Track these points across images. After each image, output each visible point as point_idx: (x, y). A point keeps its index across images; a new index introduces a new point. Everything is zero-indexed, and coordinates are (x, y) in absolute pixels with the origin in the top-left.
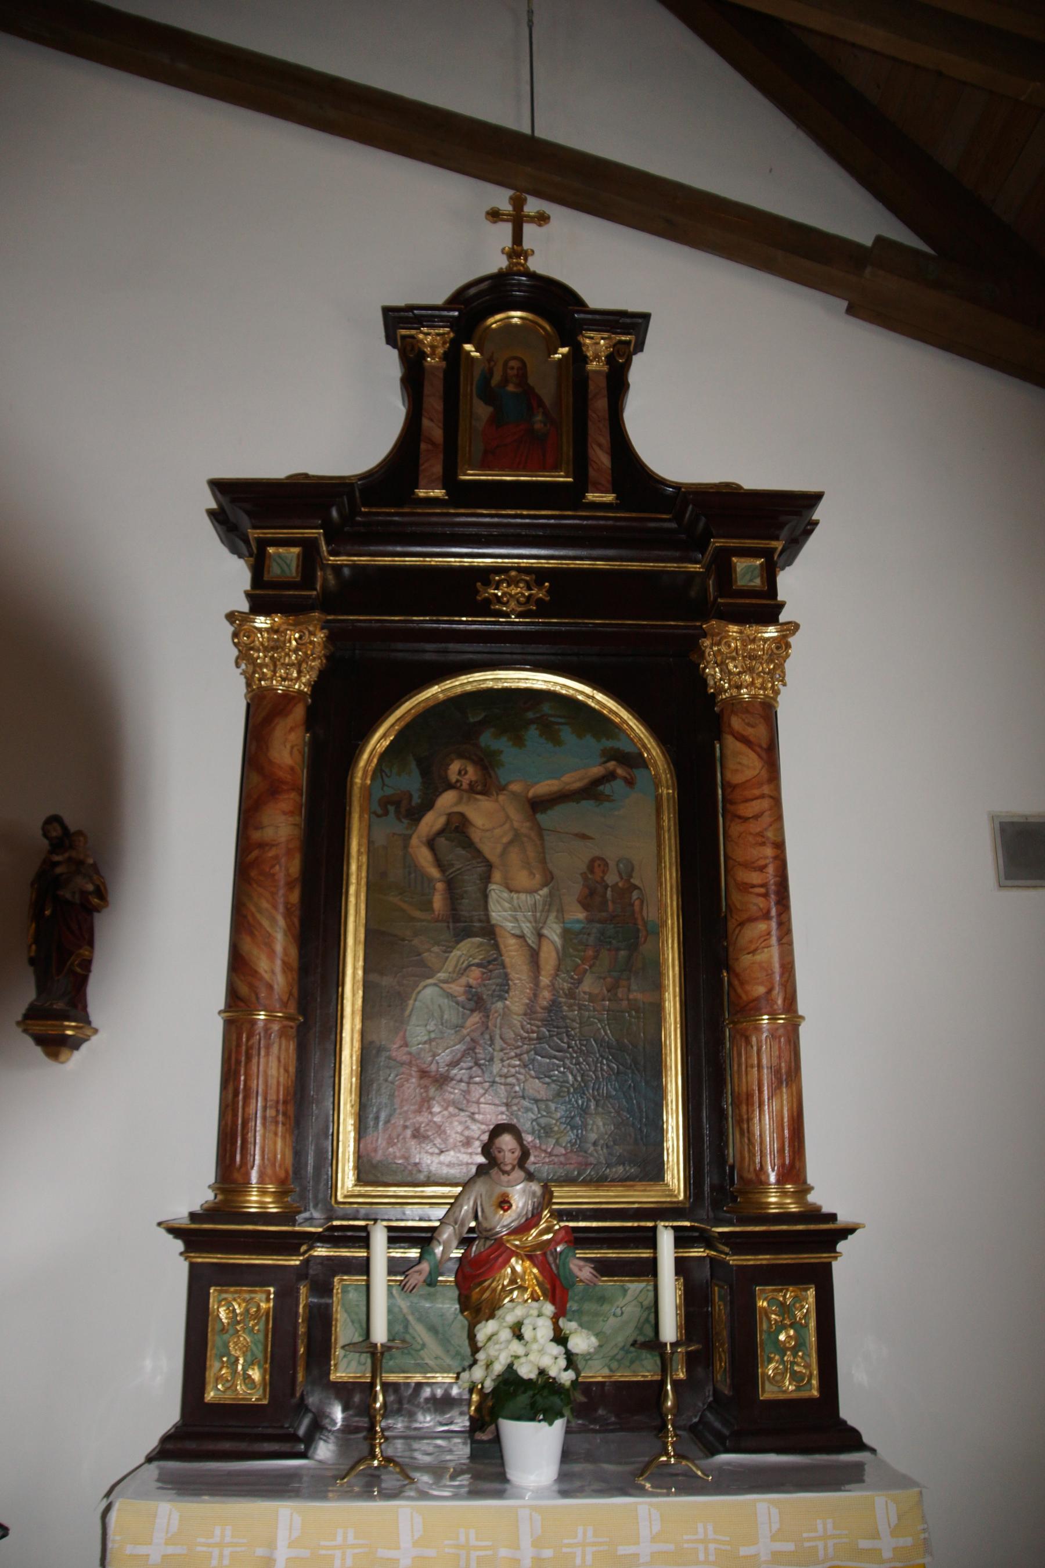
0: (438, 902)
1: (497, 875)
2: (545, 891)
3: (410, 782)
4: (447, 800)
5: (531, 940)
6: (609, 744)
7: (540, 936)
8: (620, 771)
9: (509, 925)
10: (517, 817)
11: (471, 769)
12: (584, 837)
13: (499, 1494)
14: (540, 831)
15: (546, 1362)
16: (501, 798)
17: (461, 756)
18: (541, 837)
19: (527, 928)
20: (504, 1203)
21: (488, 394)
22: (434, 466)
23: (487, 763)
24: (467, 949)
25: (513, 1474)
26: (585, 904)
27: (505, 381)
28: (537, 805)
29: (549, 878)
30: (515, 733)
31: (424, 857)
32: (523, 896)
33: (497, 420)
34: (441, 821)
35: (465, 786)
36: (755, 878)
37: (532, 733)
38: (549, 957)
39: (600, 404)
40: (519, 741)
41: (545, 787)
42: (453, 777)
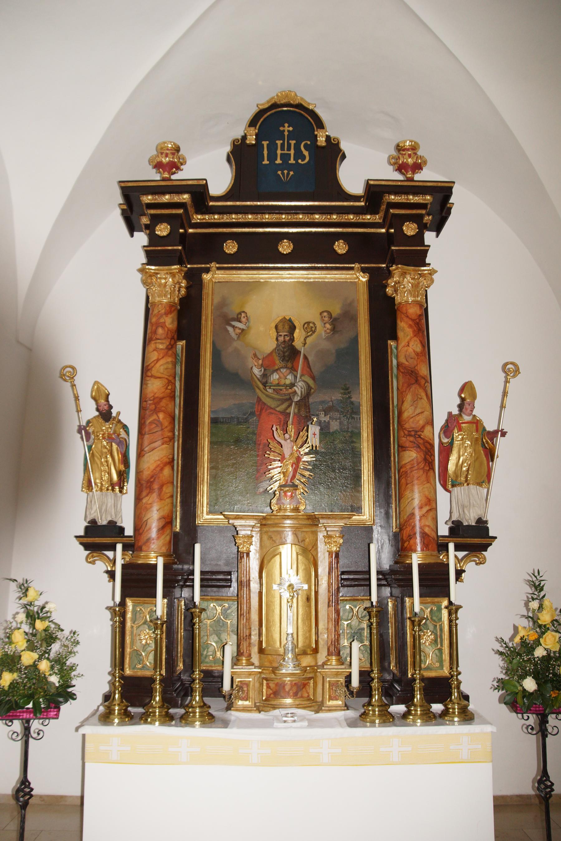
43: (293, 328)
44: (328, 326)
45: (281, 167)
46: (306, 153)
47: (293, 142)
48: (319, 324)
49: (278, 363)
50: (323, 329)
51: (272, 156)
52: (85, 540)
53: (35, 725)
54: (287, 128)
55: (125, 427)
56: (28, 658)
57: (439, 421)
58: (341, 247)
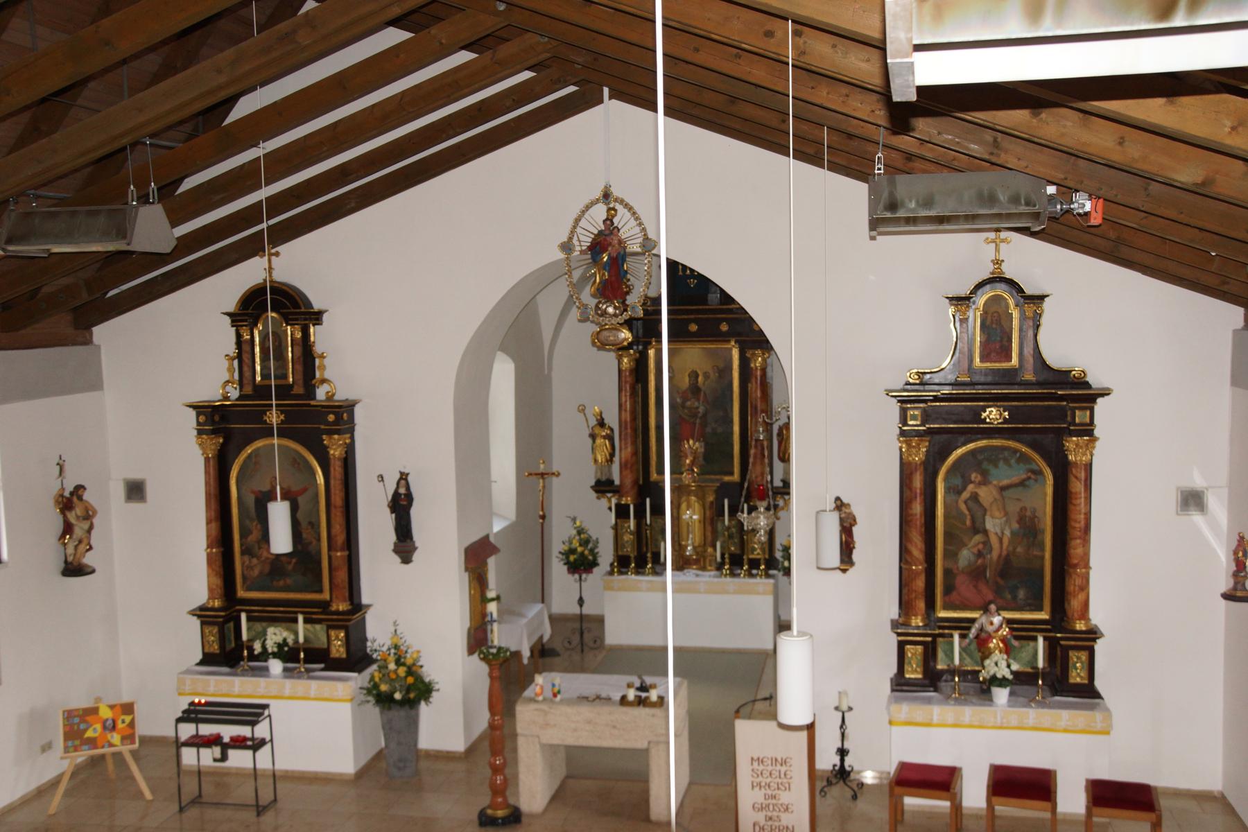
0: (968, 522)
1: (988, 513)
2: (1004, 519)
3: (957, 481)
4: (971, 487)
5: (1000, 534)
6: (1028, 466)
7: (1003, 533)
8: (1033, 476)
9: (992, 530)
10: (995, 493)
11: (979, 476)
12: (1018, 500)
13: (990, 705)
14: (1003, 498)
15: (1004, 673)
16: (990, 486)
17: (975, 471)
18: (1003, 499)
19: (999, 532)
23: (985, 474)
24: (978, 538)
25: (995, 699)
26: (1018, 522)
27: (992, 323)
28: (1003, 489)
29: (1006, 514)
31: (963, 507)
32: (997, 520)
34: (968, 495)
35: (977, 482)
36: (1077, 525)
37: (1001, 464)
38: (1006, 541)
39: (1031, 333)
40: (996, 466)
41: (1005, 482)
42: (973, 479)
43: (697, 376)
44: (717, 374)
49: (690, 395)
52: (597, 488)
53: (584, 576)
55: (612, 430)
56: (580, 549)
58: (724, 327)
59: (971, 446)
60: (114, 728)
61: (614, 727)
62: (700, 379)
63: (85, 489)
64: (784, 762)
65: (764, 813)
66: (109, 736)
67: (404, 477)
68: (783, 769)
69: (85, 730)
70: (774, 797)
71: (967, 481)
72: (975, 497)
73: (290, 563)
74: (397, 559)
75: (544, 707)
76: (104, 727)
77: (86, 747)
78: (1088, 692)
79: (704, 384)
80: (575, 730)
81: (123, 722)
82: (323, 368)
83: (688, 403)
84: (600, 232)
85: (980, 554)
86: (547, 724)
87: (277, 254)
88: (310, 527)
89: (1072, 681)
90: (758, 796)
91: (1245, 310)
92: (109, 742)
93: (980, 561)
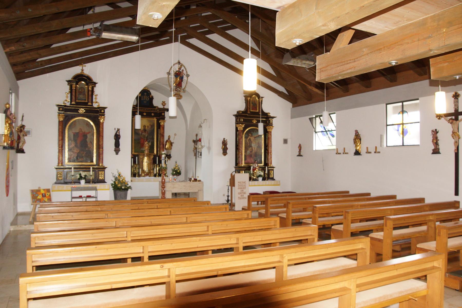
0: (249, 145)
3: (247, 135)
4: (249, 137)
7: (255, 147)
17: (250, 134)
20: (256, 165)
21: (252, 103)
22: (249, 110)
23: (252, 134)
24: (251, 148)
28: (255, 137)
29: (256, 143)
30: (253, 132)
31: (248, 141)
33: (253, 106)
37: (255, 132)
38: (256, 149)
41: (255, 136)
43: (145, 127)
45: (144, 101)
46: (148, 98)
47: (146, 96)
48: (149, 127)
50: (150, 127)
51: (143, 99)
54: (145, 94)
57: (165, 141)
58: (153, 114)
59: (249, 128)
60: (45, 196)
61: (190, 187)
62: (146, 128)
63: (25, 126)
64: (245, 183)
65: (240, 195)
66: (44, 198)
67: (118, 130)
68: (244, 184)
69: (37, 196)
70: (243, 191)
71: (248, 136)
72: (250, 139)
73: (83, 154)
74: (115, 153)
75: (173, 183)
76: (43, 196)
77: (38, 201)
78: (273, 179)
79: (147, 129)
80: (181, 188)
81: (47, 195)
82: (96, 98)
83: (143, 134)
84: (177, 71)
85: (251, 152)
86: (174, 187)
87: (85, 66)
88: (90, 143)
89: (271, 177)
90: (239, 191)
91: (293, 105)
92: (44, 200)
93: (251, 153)
